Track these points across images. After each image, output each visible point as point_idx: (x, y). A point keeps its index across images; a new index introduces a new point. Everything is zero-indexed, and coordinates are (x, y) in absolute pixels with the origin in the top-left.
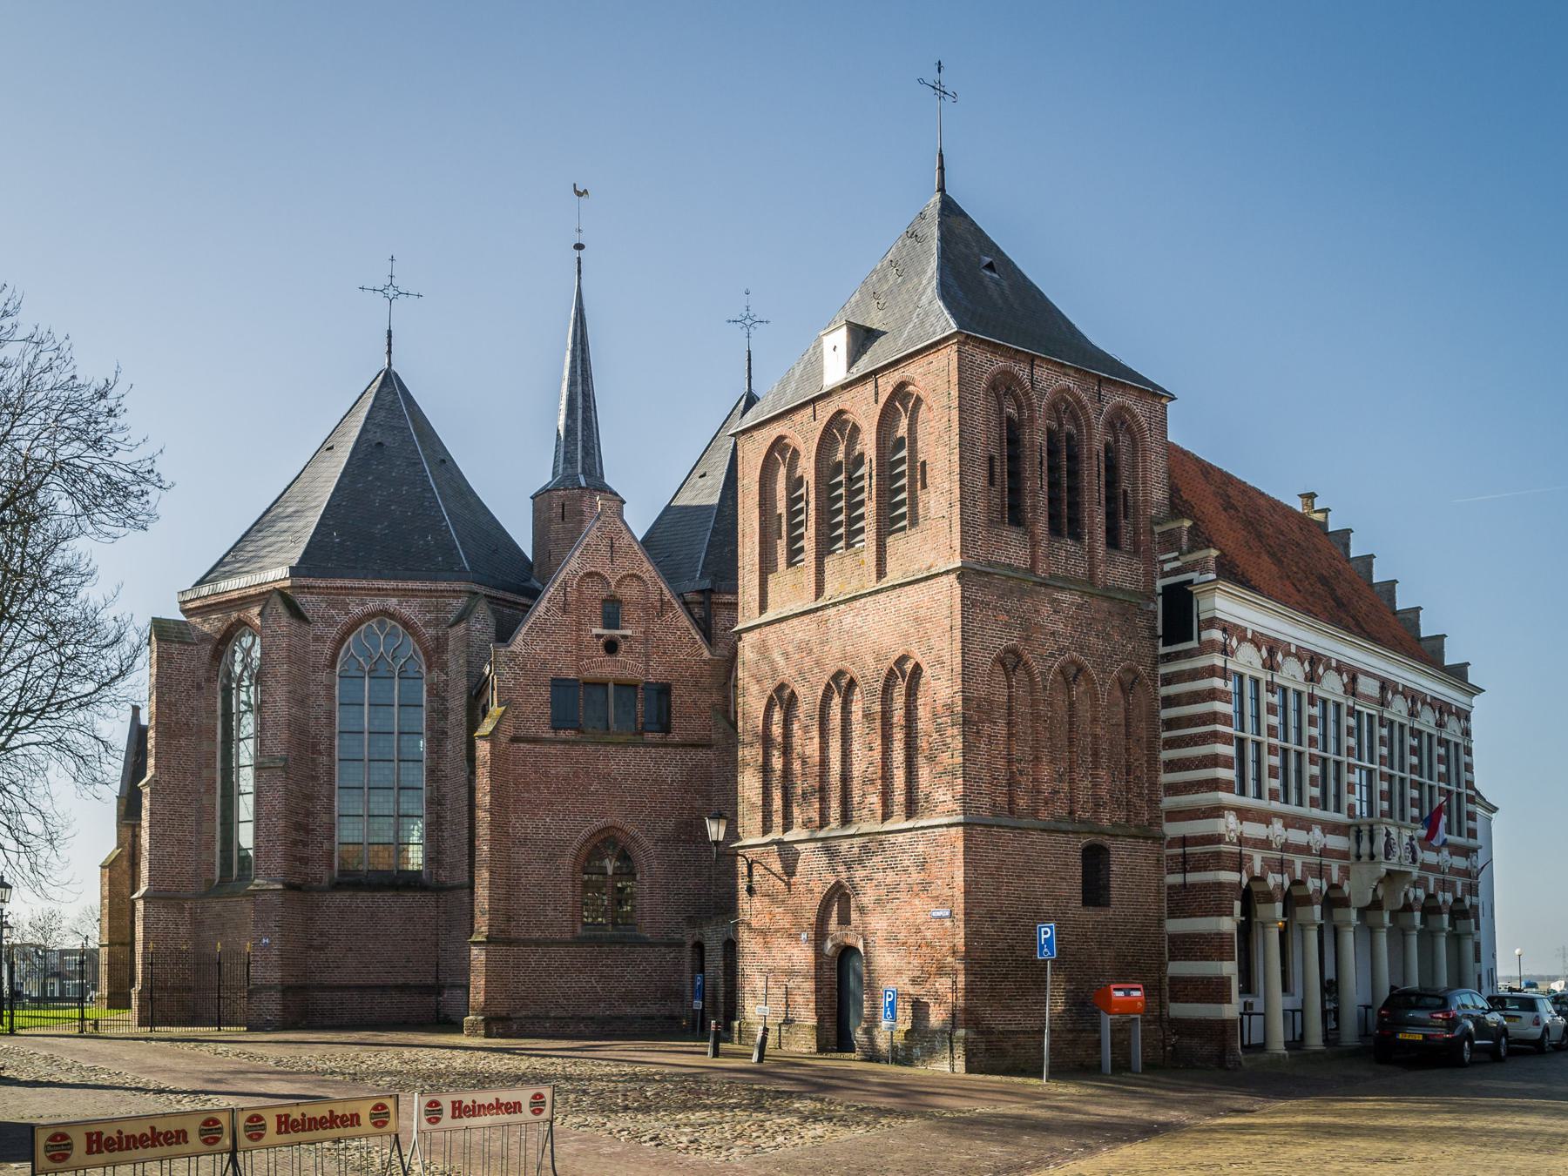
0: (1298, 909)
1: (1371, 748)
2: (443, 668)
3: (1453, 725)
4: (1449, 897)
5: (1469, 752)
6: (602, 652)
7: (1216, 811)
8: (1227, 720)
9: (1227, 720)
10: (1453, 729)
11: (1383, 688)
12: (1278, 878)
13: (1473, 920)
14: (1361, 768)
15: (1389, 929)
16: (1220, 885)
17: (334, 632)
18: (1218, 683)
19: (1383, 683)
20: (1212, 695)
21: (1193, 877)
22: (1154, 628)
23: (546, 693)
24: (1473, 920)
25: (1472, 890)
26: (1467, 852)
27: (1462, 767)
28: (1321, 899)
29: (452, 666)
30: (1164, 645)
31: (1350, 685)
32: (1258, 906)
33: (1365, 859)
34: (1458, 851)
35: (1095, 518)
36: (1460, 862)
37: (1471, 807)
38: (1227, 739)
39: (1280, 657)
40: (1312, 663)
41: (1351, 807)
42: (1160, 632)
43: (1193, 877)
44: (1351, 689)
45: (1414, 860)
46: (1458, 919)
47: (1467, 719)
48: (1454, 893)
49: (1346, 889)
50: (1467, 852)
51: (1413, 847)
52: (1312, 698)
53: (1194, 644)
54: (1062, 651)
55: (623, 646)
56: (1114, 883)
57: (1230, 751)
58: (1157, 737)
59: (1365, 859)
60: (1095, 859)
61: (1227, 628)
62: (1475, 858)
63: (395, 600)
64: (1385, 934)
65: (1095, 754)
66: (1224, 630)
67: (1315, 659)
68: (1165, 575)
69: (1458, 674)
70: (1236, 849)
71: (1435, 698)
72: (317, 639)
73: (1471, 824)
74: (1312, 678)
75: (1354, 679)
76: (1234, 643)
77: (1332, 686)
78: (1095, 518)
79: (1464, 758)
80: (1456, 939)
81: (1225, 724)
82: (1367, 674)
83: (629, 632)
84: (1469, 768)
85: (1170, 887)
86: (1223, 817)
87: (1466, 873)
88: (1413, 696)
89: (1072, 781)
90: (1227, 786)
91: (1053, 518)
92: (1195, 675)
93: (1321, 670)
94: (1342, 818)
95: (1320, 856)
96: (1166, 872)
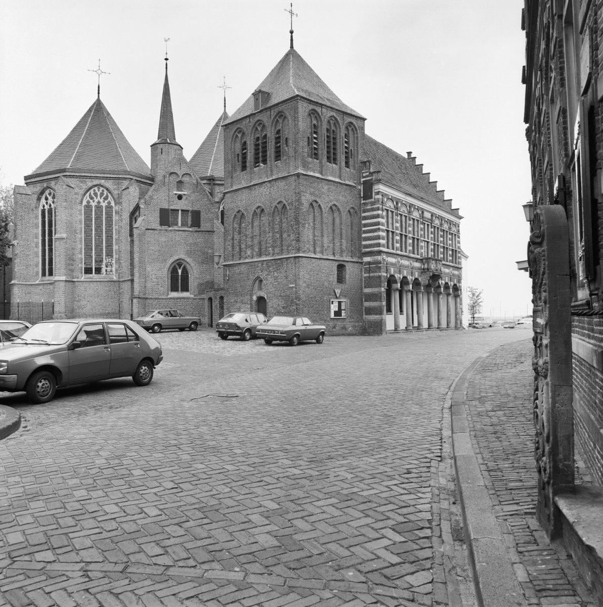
1: (428, 235)
2: (120, 203)
4: (452, 283)
5: (459, 238)
6: (177, 199)
7: (380, 252)
8: (383, 225)
9: (383, 225)
11: (432, 216)
14: (425, 241)
16: (380, 277)
17: (82, 192)
18: (380, 212)
20: (378, 216)
21: (372, 275)
22: (360, 194)
23: (158, 214)
29: (124, 205)
30: (364, 200)
35: (341, 157)
37: (459, 255)
38: (383, 231)
41: (422, 254)
42: (362, 196)
43: (372, 275)
44: (422, 216)
47: (459, 226)
52: (409, 218)
53: (373, 200)
54: (331, 201)
55: (184, 197)
56: (347, 277)
57: (384, 234)
58: (361, 230)
60: (341, 267)
61: (384, 195)
63: (103, 181)
65: (341, 235)
68: (364, 177)
69: (455, 212)
72: (76, 194)
74: (410, 212)
75: (423, 213)
76: (385, 200)
77: (416, 214)
78: (341, 157)
79: (457, 239)
82: (428, 211)
83: (186, 193)
84: (459, 242)
85: (365, 277)
88: (441, 218)
89: (334, 243)
90: (383, 246)
91: (328, 158)
92: (373, 210)
93: (412, 209)
94: (419, 257)
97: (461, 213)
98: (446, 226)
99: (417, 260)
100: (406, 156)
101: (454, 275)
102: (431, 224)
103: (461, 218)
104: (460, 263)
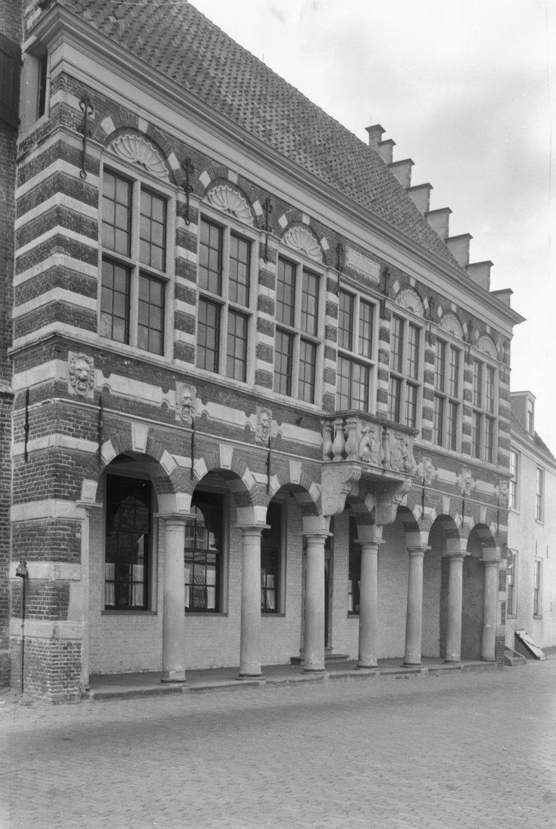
0: (238, 509)
3: (485, 345)
11: (387, 272)
12: (185, 462)
15: (467, 558)
19: (387, 269)
24: (498, 548)
25: (500, 516)
28: (269, 500)
32: (159, 497)
33: (338, 458)
34: (480, 473)
37: (503, 434)
39: (205, 179)
40: (266, 206)
47: (506, 344)
48: (477, 517)
49: (313, 490)
59: (338, 458)
62: (505, 486)
64: (376, 552)
66: (85, 100)
67: (272, 205)
69: (500, 302)
74: (266, 225)
76: (108, 125)
77: (300, 244)
80: (476, 568)
81: (78, 229)
86: (65, 358)
87: (494, 500)
90: (84, 319)
96: (13, 441)
97: (516, 304)
98: (450, 328)
99: (301, 418)
100: (364, 138)
101: (476, 494)
102: (382, 303)
103: (516, 319)
104: (504, 461)
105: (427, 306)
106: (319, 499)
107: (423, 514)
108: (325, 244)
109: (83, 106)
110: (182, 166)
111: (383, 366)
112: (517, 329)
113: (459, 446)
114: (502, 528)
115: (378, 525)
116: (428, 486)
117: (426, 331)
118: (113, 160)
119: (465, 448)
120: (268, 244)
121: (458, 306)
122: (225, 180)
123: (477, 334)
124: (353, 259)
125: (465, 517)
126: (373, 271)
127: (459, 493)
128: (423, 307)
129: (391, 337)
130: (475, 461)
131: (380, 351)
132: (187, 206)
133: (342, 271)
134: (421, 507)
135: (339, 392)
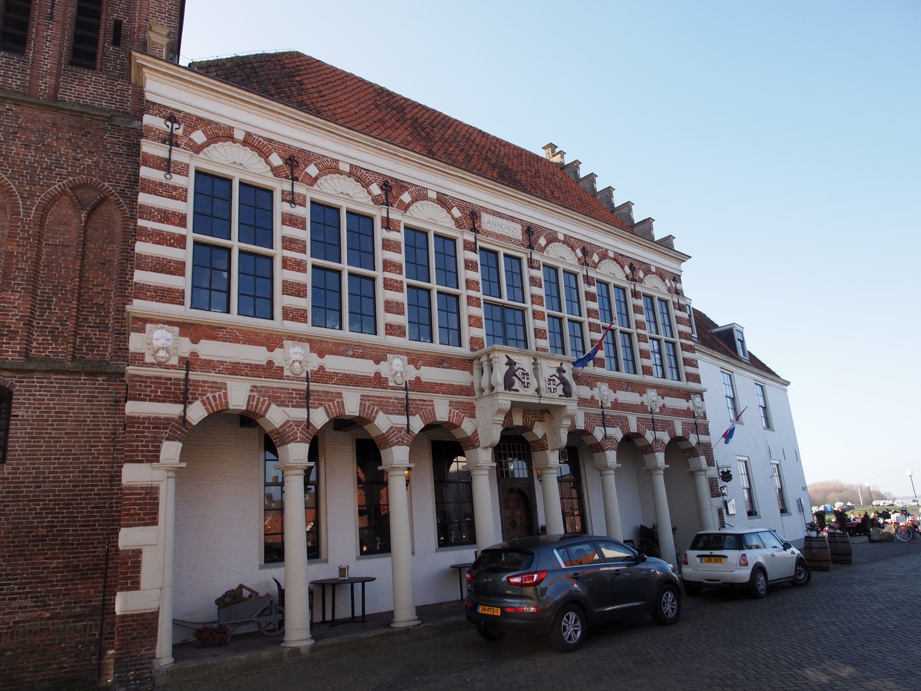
10: (652, 285)
13: (703, 459)
26: (687, 395)
27: (674, 321)
31: (467, 223)
33: (487, 392)
36: (680, 404)
37: (688, 355)
45: (567, 393)
46: (689, 457)
47: (676, 278)
50: (687, 395)
51: (564, 382)
59: (487, 392)
70: (181, 374)
71: (621, 255)
73: (690, 370)
76: (199, 137)
87: (689, 413)
95: (406, 389)
103: (682, 258)
104: (696, 378)
105: (580, 255)
106: (475, 433)
107: (605, 434)
108: (456, 213)
109: (169, 124)
110: (286, 163)
111: (538, 308)
112: (684, 266)
113: (640, 369)
114: (703, 438)
115: (553, 450)
116: (657, 413)
117: (584, 276)
118: (236, 171)
119: (647, 371)
120: (390, 217)
121: (615, 253)
122: (425, 198)
123: (641, 274)
124: (487, 222)
125: (656, 432)
126: (517, 232)
127: (647, 412)
128: (576, 255)
129: (543, 283)
130: (614, 374)
131: (532, 296)
132: (292, 193)
133: (478, 232)
134: (602, 428)
135: (608, 355)
